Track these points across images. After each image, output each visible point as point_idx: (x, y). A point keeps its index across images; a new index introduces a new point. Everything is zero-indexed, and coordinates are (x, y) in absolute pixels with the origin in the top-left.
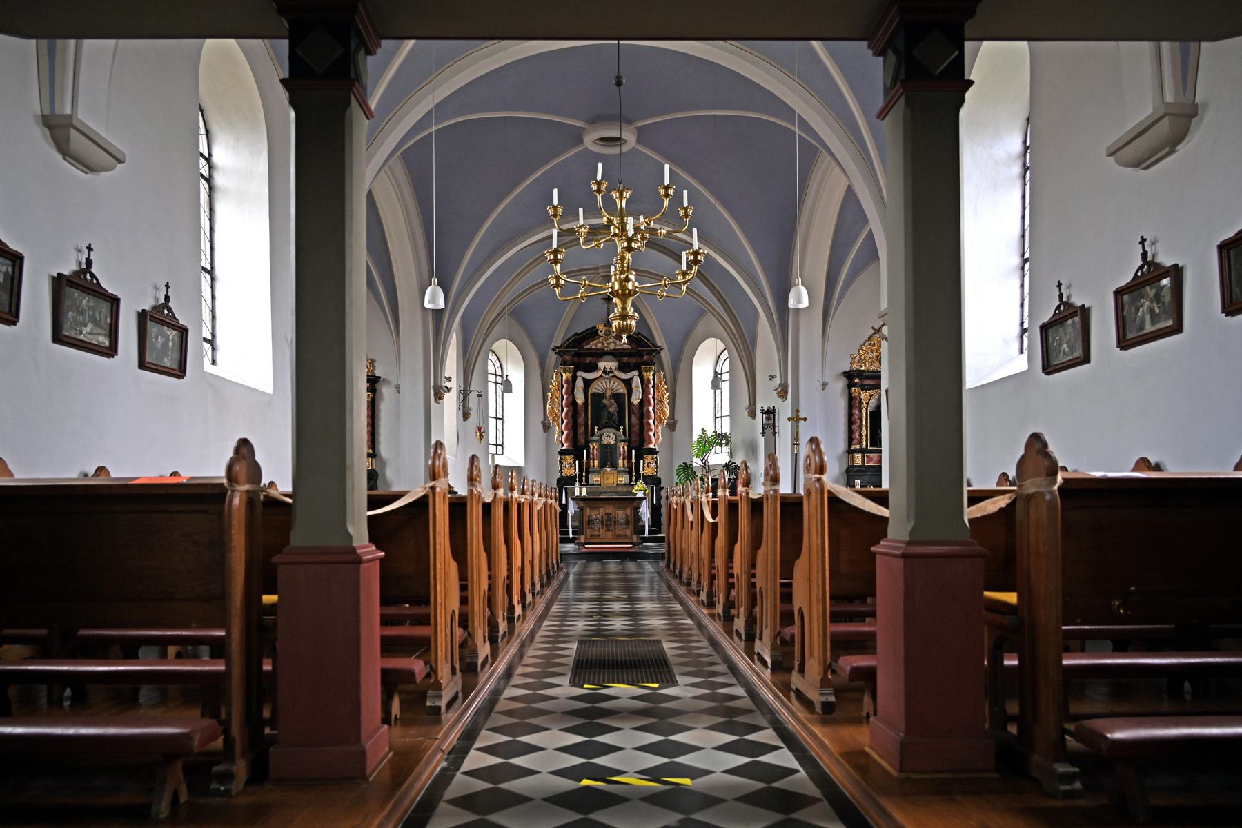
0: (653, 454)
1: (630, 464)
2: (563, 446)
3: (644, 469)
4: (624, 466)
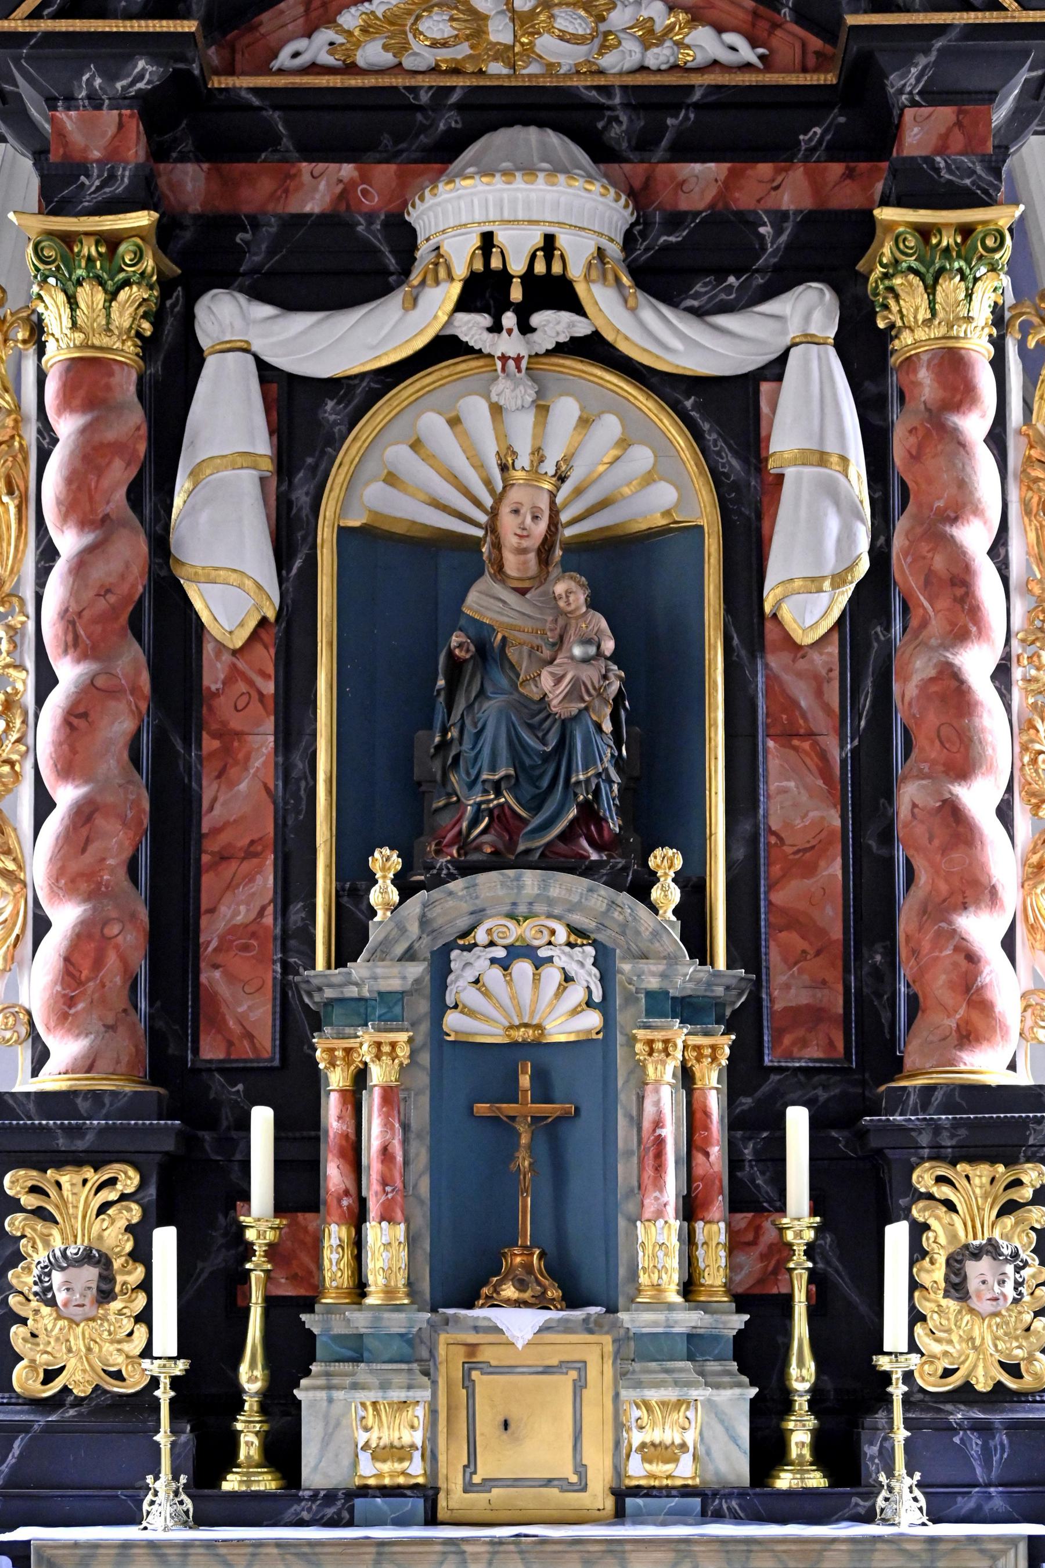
0: (1010, 1162)
1: (751, 1263)
2: (41, 1057)
3: (916, 1317)
4: (689, 1288)
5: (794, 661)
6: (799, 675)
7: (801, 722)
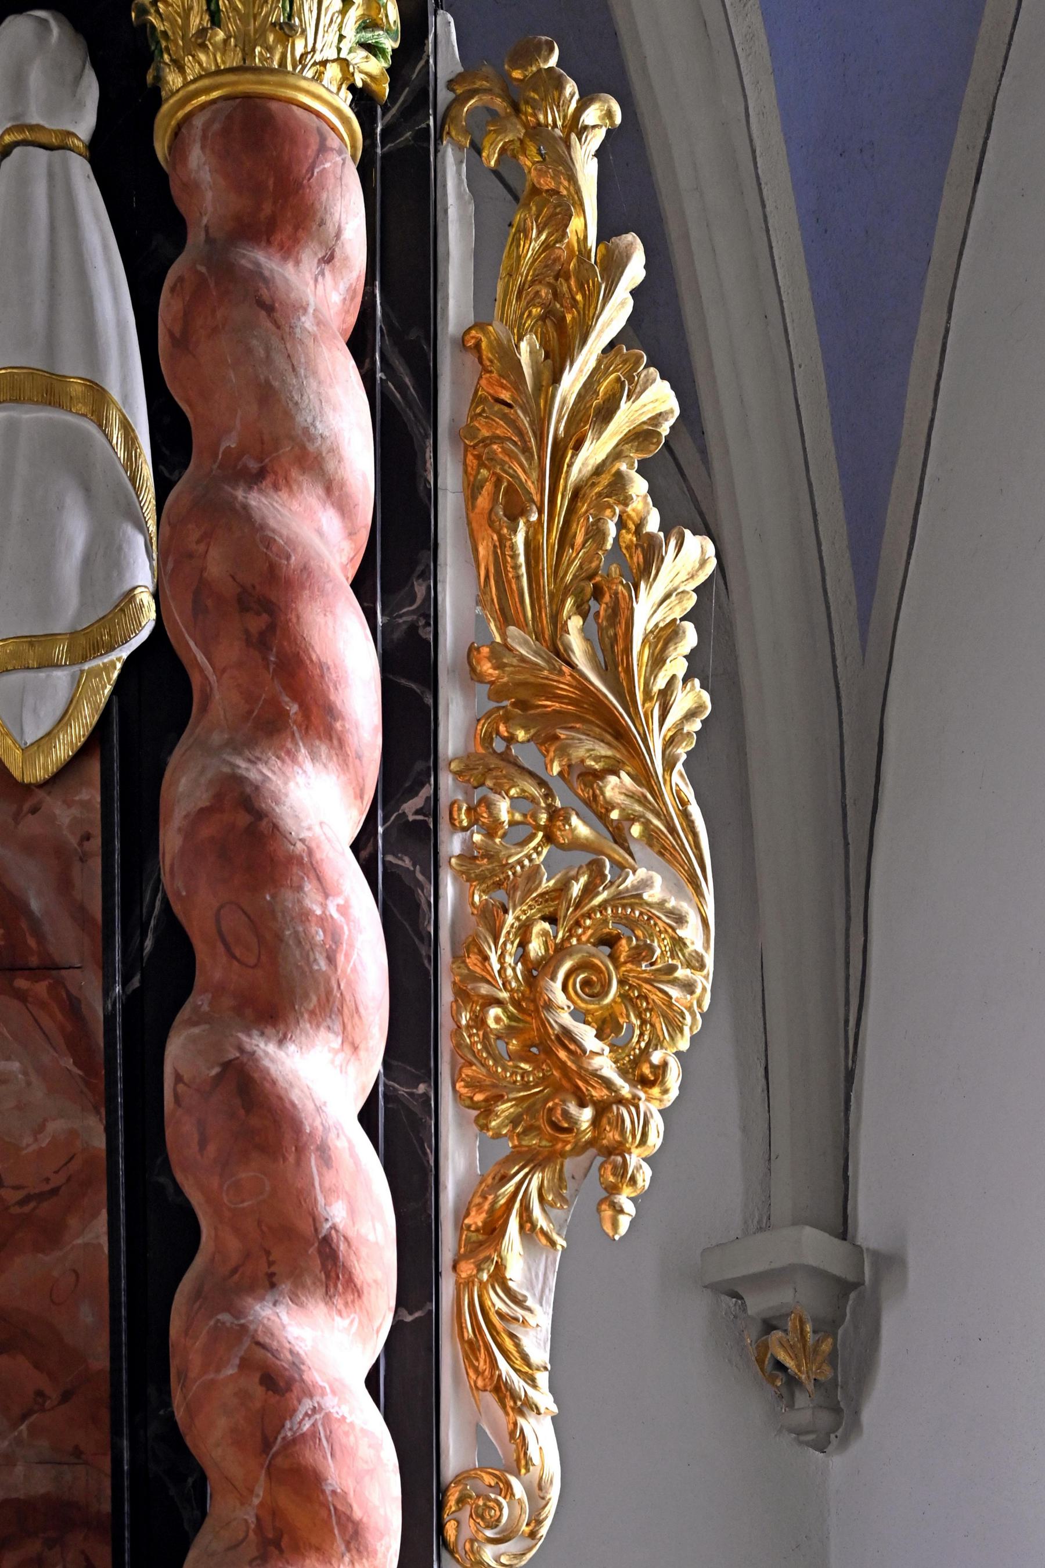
5: (17, 817)
6: (29, 847)
7: (32, 942)
